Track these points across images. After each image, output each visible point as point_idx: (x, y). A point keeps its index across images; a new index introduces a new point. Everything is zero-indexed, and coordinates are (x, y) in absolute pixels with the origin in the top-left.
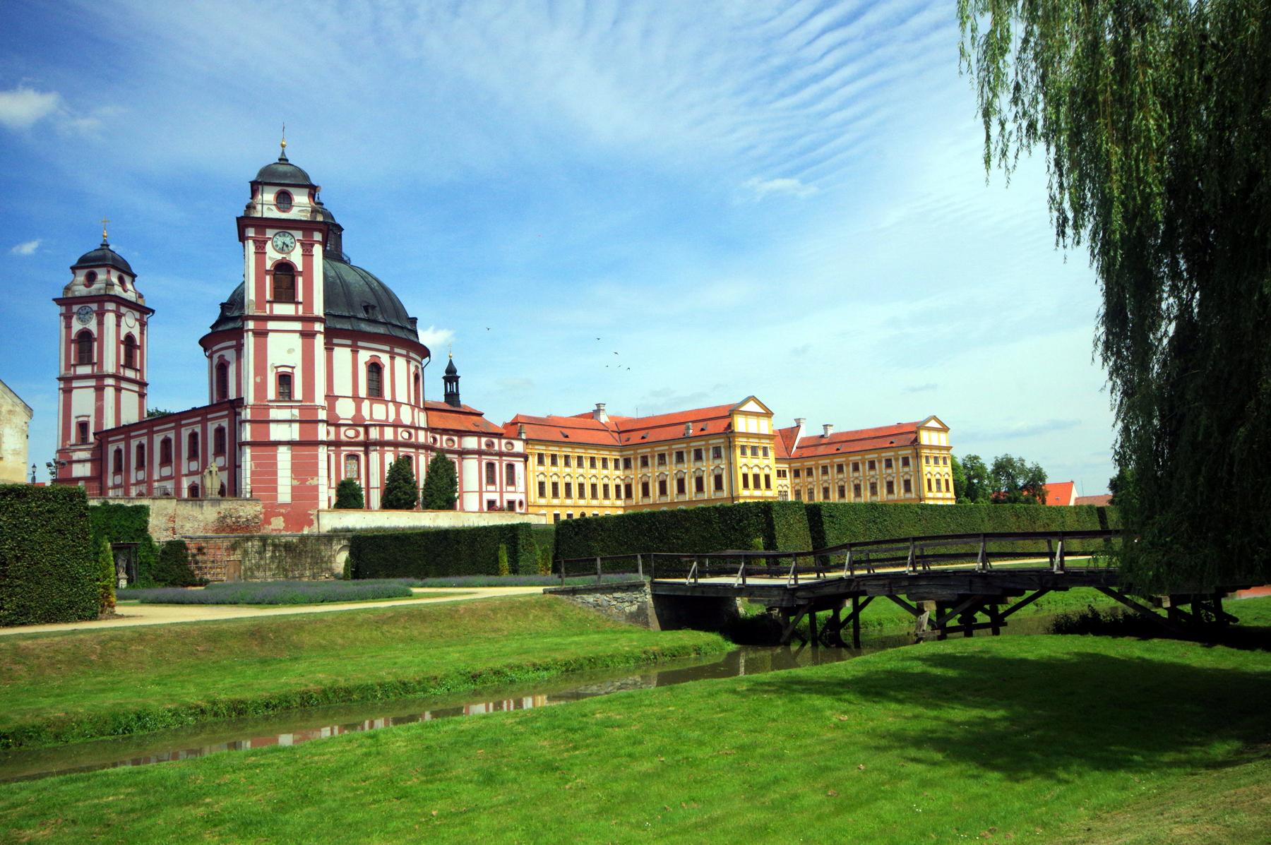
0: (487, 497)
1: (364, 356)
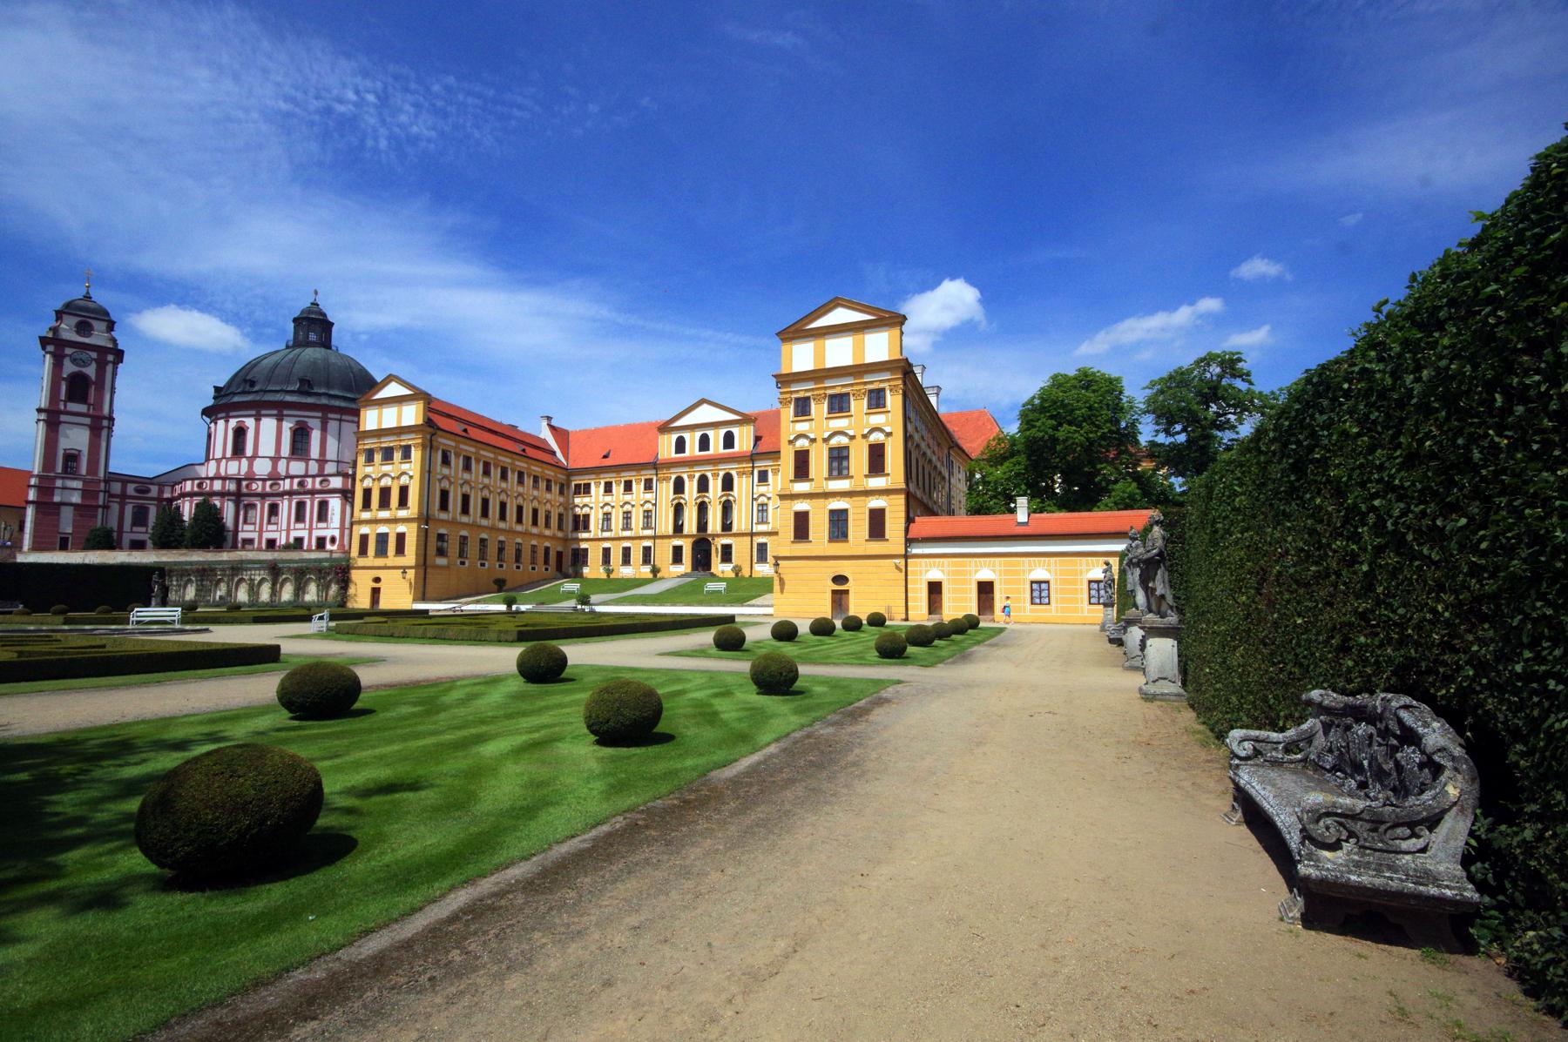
0: (294, 534)
1: (233, 423)
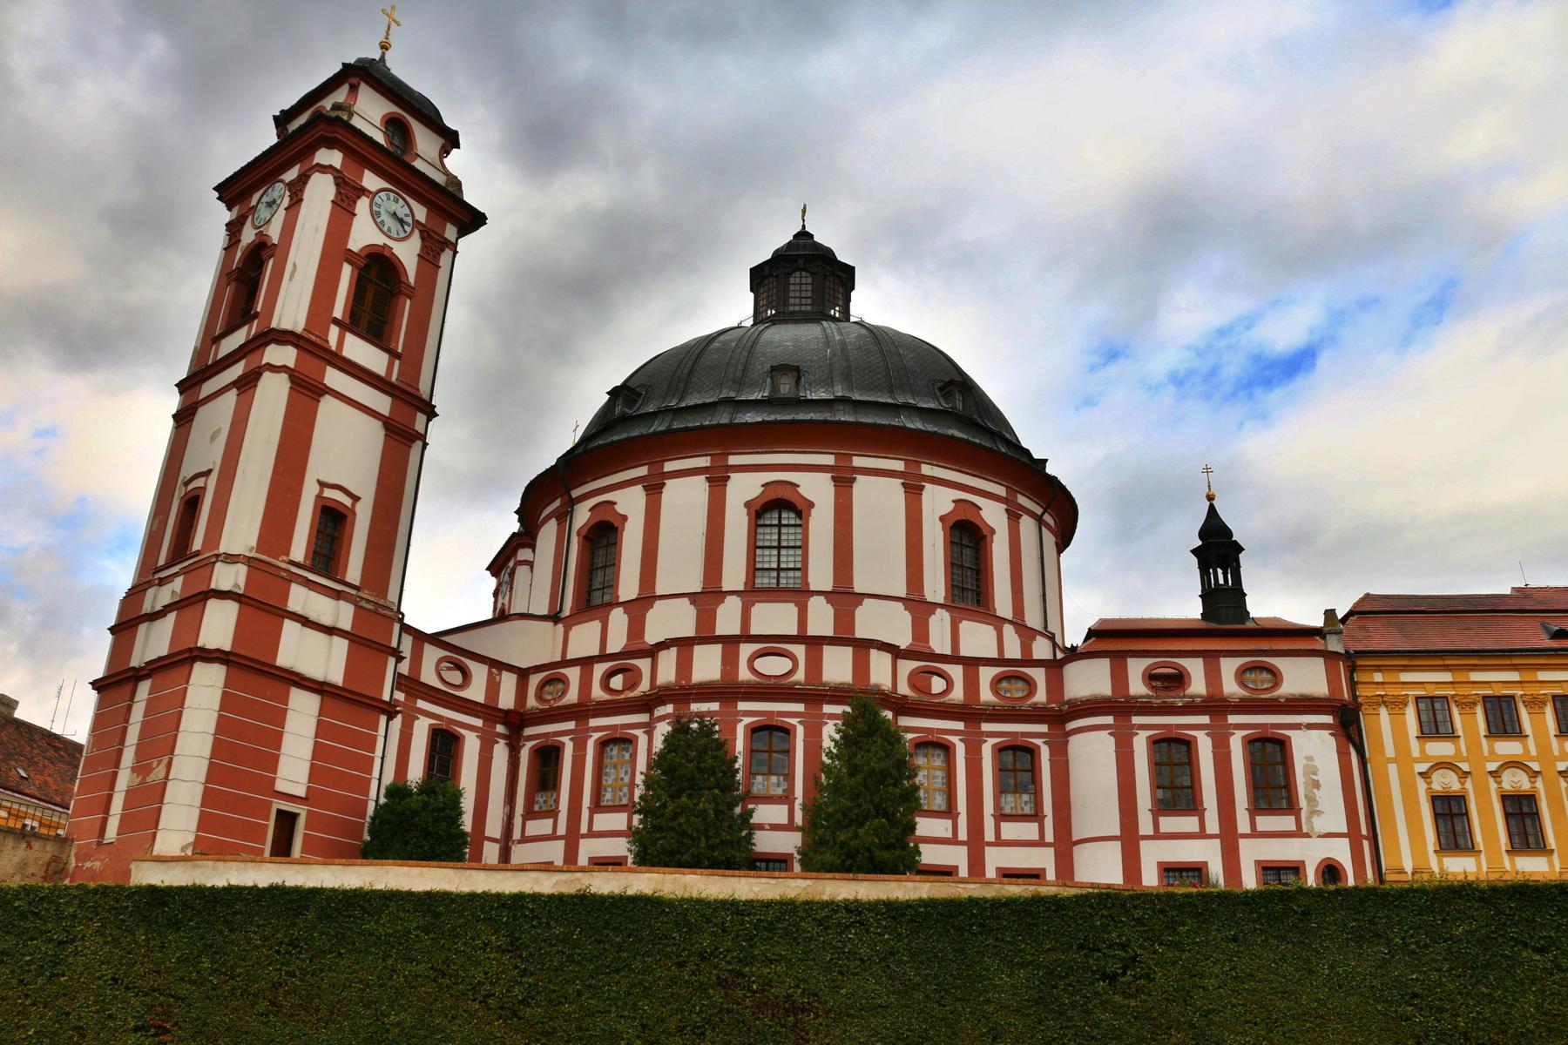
0: (1153, 855)
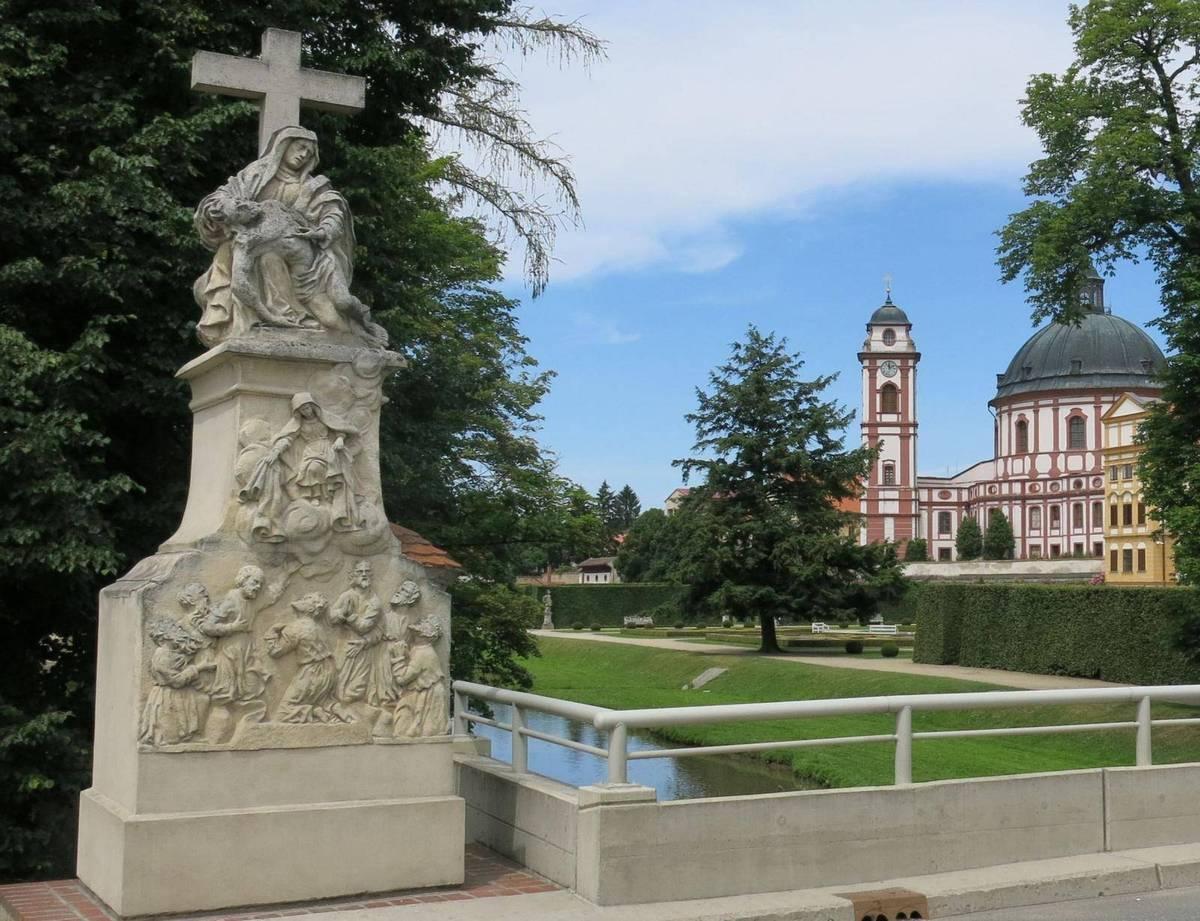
0: (1075, 540)
